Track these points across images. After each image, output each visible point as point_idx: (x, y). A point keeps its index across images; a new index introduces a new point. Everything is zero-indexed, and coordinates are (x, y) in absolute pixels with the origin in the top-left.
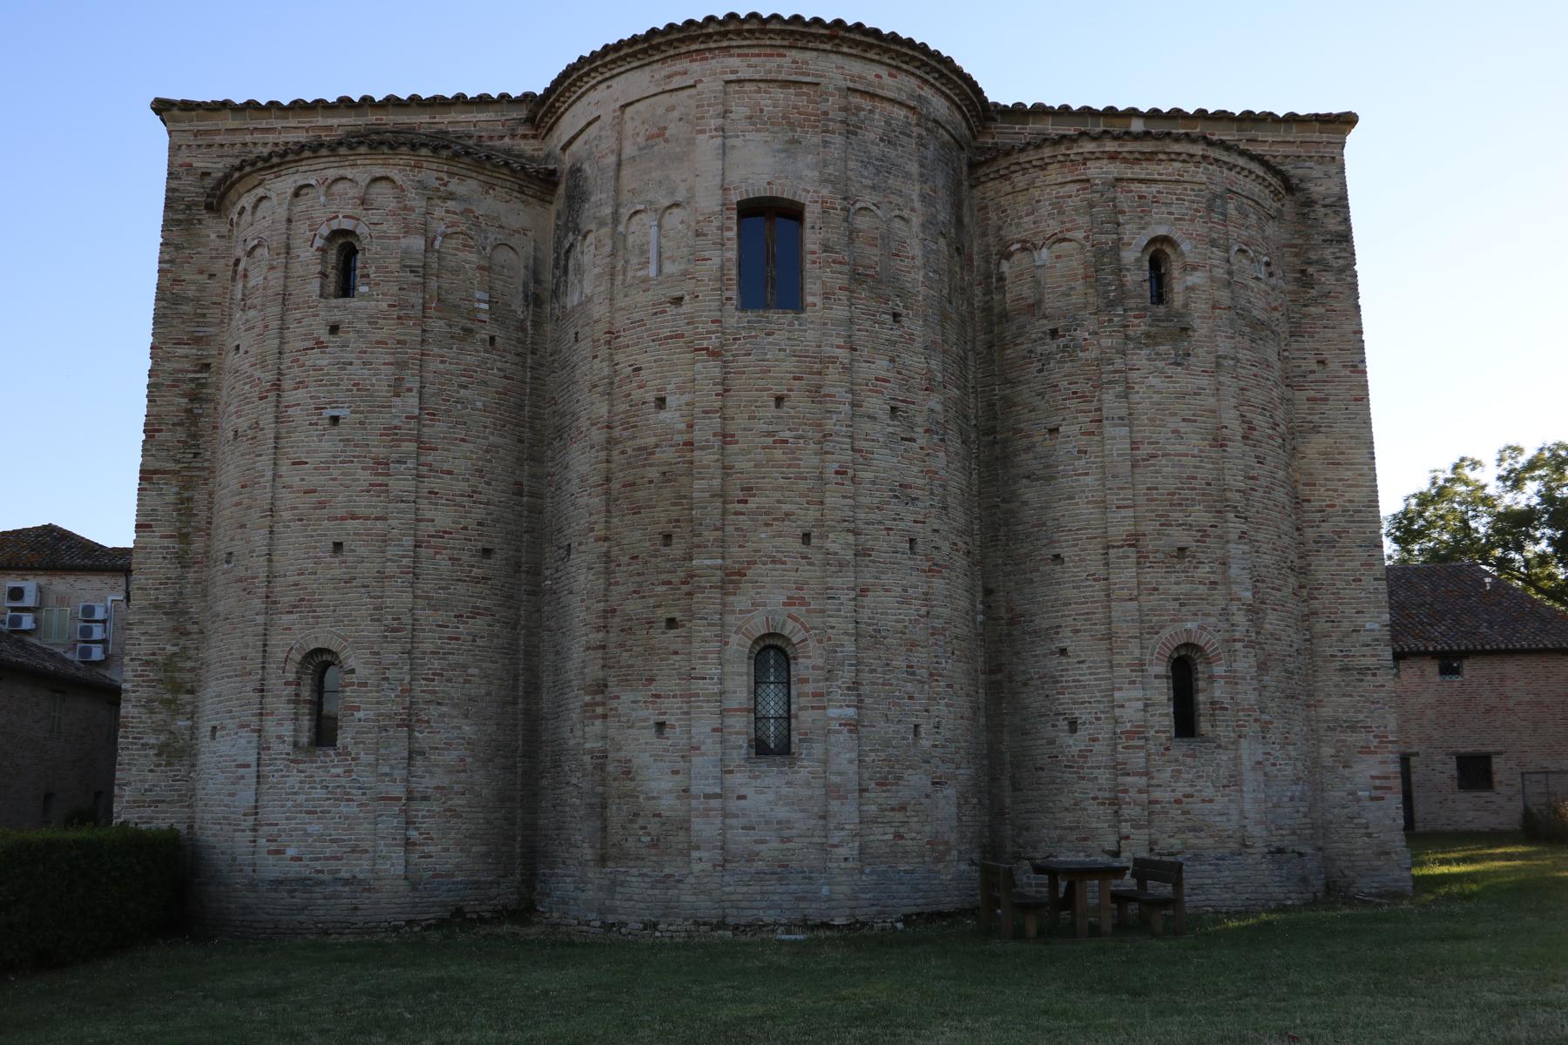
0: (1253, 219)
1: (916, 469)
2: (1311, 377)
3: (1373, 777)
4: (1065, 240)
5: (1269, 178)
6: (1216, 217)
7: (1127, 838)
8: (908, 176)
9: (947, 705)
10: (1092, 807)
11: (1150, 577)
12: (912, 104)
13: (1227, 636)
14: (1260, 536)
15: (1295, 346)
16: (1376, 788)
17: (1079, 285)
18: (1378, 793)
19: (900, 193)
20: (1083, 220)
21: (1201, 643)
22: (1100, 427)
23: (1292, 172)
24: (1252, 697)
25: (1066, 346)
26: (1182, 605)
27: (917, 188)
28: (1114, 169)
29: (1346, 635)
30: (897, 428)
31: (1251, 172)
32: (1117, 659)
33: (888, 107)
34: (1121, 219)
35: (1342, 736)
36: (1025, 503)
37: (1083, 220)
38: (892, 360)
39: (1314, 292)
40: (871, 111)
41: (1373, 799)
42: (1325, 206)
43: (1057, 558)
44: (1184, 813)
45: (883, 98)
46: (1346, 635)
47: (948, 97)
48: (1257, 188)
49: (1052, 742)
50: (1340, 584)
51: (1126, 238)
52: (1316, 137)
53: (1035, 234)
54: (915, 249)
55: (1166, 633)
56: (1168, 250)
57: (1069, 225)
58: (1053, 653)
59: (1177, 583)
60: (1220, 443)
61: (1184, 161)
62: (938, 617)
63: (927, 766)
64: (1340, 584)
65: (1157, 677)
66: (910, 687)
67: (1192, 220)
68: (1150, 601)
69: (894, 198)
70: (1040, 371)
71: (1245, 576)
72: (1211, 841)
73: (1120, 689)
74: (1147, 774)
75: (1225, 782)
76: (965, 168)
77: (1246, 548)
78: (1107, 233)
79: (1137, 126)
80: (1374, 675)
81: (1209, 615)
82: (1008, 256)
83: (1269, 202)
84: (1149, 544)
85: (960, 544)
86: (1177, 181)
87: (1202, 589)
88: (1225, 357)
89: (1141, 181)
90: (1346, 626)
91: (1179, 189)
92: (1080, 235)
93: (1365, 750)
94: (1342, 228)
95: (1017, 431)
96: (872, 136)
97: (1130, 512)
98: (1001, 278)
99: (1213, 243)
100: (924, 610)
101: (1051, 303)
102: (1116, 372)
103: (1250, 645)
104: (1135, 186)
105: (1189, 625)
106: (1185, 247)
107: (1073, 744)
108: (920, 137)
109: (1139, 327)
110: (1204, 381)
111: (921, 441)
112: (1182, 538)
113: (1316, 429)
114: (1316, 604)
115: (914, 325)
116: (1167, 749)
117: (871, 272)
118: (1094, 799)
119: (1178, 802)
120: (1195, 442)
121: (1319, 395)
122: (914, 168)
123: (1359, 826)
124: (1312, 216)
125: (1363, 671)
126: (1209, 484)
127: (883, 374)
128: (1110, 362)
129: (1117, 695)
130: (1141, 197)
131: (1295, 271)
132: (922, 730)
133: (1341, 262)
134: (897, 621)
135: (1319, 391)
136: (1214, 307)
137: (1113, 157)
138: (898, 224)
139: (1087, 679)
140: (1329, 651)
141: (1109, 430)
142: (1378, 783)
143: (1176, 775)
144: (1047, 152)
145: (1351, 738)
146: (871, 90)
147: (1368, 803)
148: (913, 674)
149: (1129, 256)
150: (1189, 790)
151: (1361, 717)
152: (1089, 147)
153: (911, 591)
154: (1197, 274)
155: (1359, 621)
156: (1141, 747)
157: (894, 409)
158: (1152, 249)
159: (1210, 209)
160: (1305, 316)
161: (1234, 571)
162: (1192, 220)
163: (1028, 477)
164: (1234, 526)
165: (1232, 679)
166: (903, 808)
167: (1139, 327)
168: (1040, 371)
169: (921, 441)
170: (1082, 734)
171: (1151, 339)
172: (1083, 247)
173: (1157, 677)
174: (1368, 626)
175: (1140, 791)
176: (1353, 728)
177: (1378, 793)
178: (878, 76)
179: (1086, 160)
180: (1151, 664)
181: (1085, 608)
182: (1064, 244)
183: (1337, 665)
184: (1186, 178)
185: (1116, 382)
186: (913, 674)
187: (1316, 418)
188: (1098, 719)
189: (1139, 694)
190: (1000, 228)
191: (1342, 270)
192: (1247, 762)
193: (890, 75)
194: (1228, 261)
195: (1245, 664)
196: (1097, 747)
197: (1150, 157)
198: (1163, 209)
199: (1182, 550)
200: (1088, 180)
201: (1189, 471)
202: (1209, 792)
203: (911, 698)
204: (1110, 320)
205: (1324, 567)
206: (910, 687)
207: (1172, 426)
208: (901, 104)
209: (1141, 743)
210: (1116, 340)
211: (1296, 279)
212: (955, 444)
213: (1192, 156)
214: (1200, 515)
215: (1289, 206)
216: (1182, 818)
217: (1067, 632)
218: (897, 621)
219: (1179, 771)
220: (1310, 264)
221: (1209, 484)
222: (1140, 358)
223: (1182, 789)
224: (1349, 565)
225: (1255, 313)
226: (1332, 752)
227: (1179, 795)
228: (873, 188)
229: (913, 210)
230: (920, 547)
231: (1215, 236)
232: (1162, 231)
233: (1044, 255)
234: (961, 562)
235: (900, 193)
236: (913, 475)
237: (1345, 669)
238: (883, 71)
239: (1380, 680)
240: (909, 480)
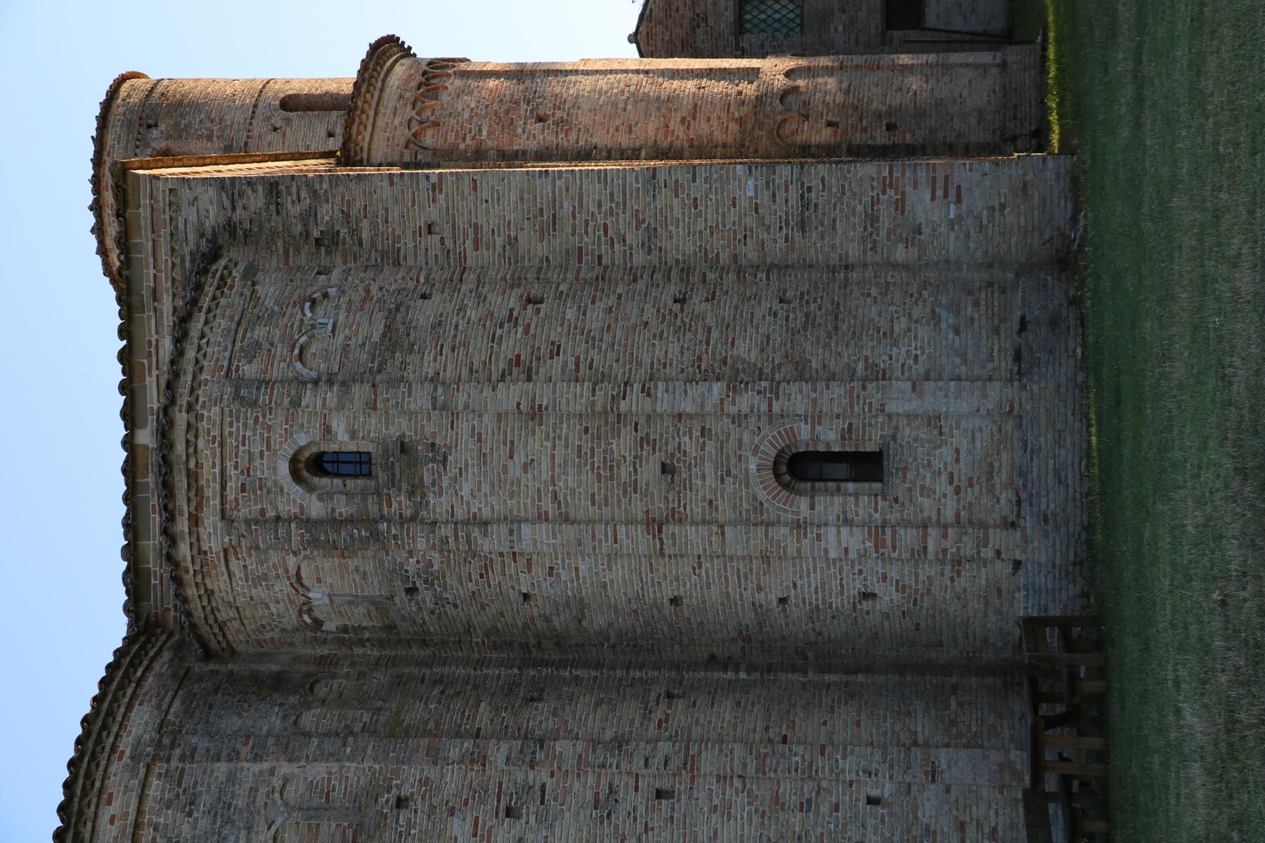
0: (260, 332)
1: (576, 786)
2: (449, 243)
3: (933, 198)
4: (298, 574)
5: (206, 302)
6: (263, 398)
7: (998, 552)
8: (231, 778)
9: (844, 757)
10: (962, 582)
11: (696, 509)
12: (143, 771)
13: (764, 419)
14: (647, 359)
15: (410, 261)
16: (946, 196)
17: (352, 563)
18: (952, 192)
19: (254, 790)
20: (274, 557)
21: (773, 453)
22: (522, 554)
23: (192, 246)
24: (837, 390)
25: (426, 582)
26: (729, 474)
27: (246, 765)
28: (210, 520)
29: (761, 221)
30: (531, 809)
31: (203, 336)
32: (791, 551)
33: (149, 804)
34: (271, 514)
35: (883, 233)
36: (610, 625)
37: (274, 557)
38: (452, 812)
39: (344, 232)
40: (156, 829)
41: (959, 200)
42: (234, 208)
43: (675, 601)
44: (971, 485)
45: (139, 812)
46: (761, 221)
47: (129, 707)
48: (222, 323)
49: (887, 616)
50: (700, 225)
51: (295, 510)
52: (144, 212)
53: (291, 602)
54: (318, 771)
55: (762, 495)
56: (306, 454)
57: (280, 571)
58: (785, 610)
59: (704, 478)
60: (536, 413)
61: (196, 437)
62: (745, 765)
63: (914, 788)
64: (700, 225)
65: (812, 508)
66: (824, 809)
67: (269, 428)
68: (725, 511)
69: (260, 800)
70: (455, 606)
71: (695, 390)
72: (1004, 455)
73: (826, 551)
74: (925, 527)
75: (936, 432)
76: (212, 666)
77: (661, 385)
78: (289, 534)
79: (145, 437)
80: (809, 189)
81: (740, 441)
82: (318, 623)
83: (233, 300)
84: (659, 507)
85: (658, 715)
86: (222, 444)
87: (711, 447)
88: (434, 399)
89: (223, 488)
90: (750, 221)
91: (230, 442)
92: (292, 561)
93: (900, 205)
94: (260, 189)
95: (526, 625)
96: (186, 828)
97: (622, 529)
98: (345, 629)
99: (296, 403)
100: (737, 783)
101: (375, 588)
102: (456, 535)
103: (775, 391)
104: (231, 495)
105: (753, 467)
106: (302, 440)
107: (888, 597)
108: (182, 759)
109: (401, 503)
110: (464, 426)
111: (544, 776)
112: (649, 471)
113: (513, 242)
114: (725, 257)
115: (409, 778)
116: (896, 500)
117: (350, 833)
118: (952, 580)
119: (957, 491)
120: (537, 445)
121: (471, 236)
122: (222, 768)
123: (991, 219)
124: (246, 225)
125: (805, 204)
126: (586, 430)
127: (469, 826)
128: (445, 541)
129: (833, 554)
130: (243, 490)
131: (318, 252)
132: (875, 793)
133: (303, 194)
134: (750, 821)
135: (465, 235)
136: (375, 408)
137: (195, 521)
138: (290, 794)
139: (815, 580)
140: (781, 243)
141: (525, 546)
142: (939, 193)
143: (926, 491)
144: (191, 592)
145: (885, 222)
146: (129, 830)
147: (964, 206)
148: (809, 802)
149: (316, 508)
150: (944, 477)
151: (859, 208)
152: (184, 550)
153: (716, 801)
154: (334, 425)
155: (744, 203)
156: (894, 532)
157: (509, 813)
158: (305, 473)
159: (254, 404)
160: (373, 244)
161: (688, 407)
162: (269, 428)
163: (580, 621)
164: (634, 403)
165: (815, 418)
166: (962, 827)
167: (401, 503)
168: (455, 606)
169: (544, 776)
170: (878, 589)
171: (415, 489)
172: (306, 557)
173: (812, 508)
174: (751, 193)
175: (945, 536)
176: (873, 219)
177: (952, 192)
178: (112, 822)
179: (200, 552)
180: (798, 513)
181: (733, 578)
182: (303, 574)
183: (797, 235)
184: (217, 433)
185: (468, 536)
186: (809, 802)
187: (499, 241)
188: (860, 572)
189: (832, 531)
190: (284, 630)
191: (314, 194)
192: (913, 405)
193: (109, 803)
194: (316, 383)
195: (797, 398)
196: (893, 574)
197: (193, 477)
198: (257, 463)
199: (665, 469)
200: (225, 551)
201: (572, 455)
202: (946, 453)
203: (837, 809)
204: (395, 537)
205: (680, 244)
206: (824, 809)
207: (519, 471)
208: (144, 785)
209: (888, 531)
210: (418, 531)
211: (328, 253)
212: (540, 718)
213: (189, 425)
214: (623, 444)
215: (237, 257)
216: (977, 487)
217: (760, 598)
218: (750, 821)
219: (923, 488)
220: (306, 234)
221: (586, 430)
222: (439, 505)
223: (942, 486)
224: (677, 213)
225: (376, 338)
226: (901, 246)
227: (950, 490)
228: (249, 828)
229: (272, 772)
230: (665, 784)
231: (286, 401)
232: (284, 468)
233: (317, 595)
234: (680, 714)
235: (254, 790)
236: (583, 788)
237: (803, 226)
238: (106, 813)
239: (816, 183)
240: (589, 796)
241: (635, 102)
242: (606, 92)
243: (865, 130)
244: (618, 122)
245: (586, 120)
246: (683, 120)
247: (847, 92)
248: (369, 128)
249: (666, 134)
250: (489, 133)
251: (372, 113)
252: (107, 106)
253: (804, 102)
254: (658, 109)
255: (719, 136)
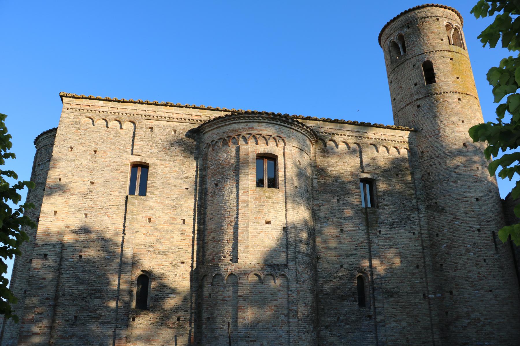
241: (221, 217)
242: (226, 205)
243: (207, 309)
244: (214, 214)
245: (215, 202)
246: (214, 238)
247: (223, 300)
248: (211, 129)
249: (210, 233)
250: (211, 169)
251: (216, 126)
252: (410, 10)
253: (219, 283)
254: (218, 227)
255: (208, 252)
